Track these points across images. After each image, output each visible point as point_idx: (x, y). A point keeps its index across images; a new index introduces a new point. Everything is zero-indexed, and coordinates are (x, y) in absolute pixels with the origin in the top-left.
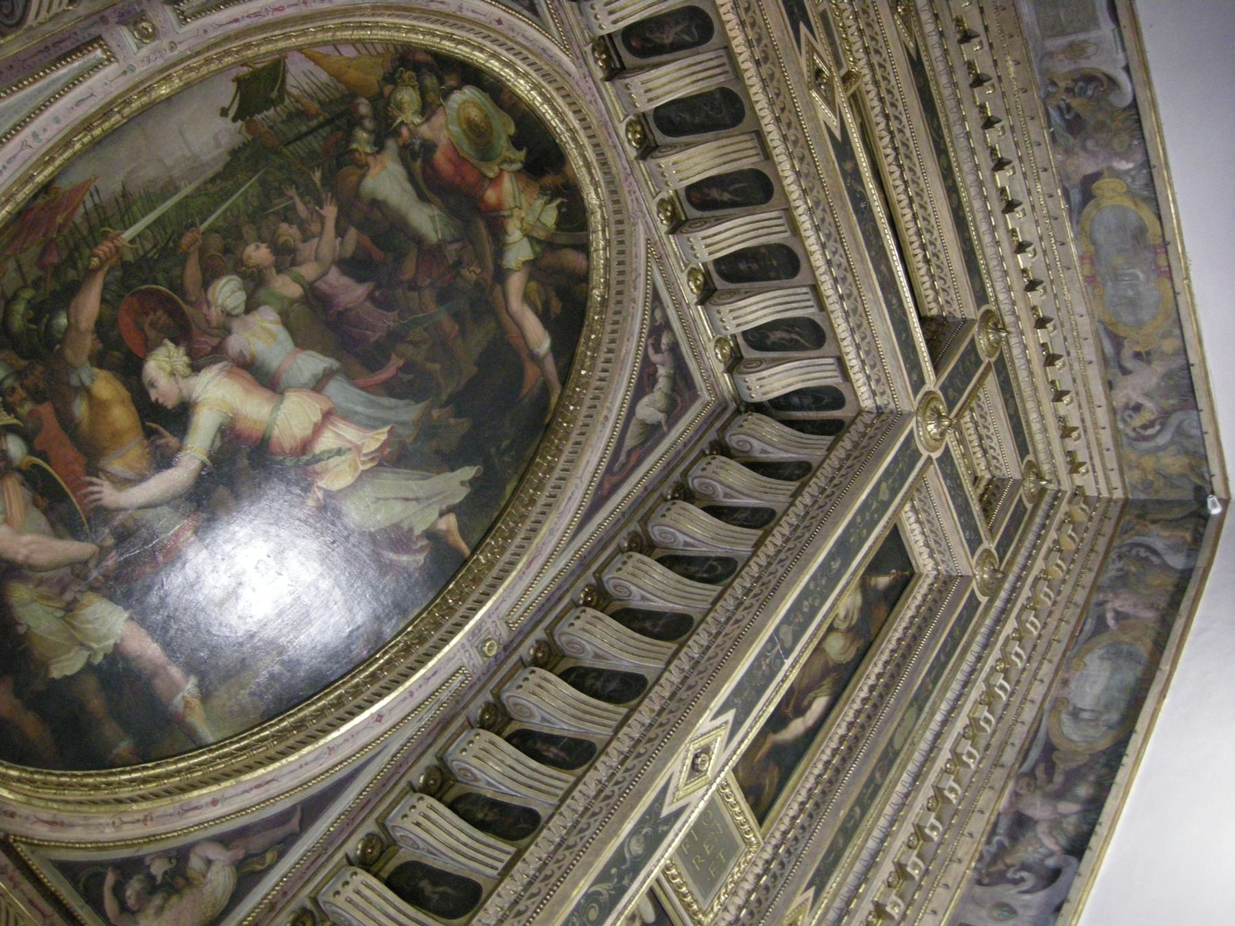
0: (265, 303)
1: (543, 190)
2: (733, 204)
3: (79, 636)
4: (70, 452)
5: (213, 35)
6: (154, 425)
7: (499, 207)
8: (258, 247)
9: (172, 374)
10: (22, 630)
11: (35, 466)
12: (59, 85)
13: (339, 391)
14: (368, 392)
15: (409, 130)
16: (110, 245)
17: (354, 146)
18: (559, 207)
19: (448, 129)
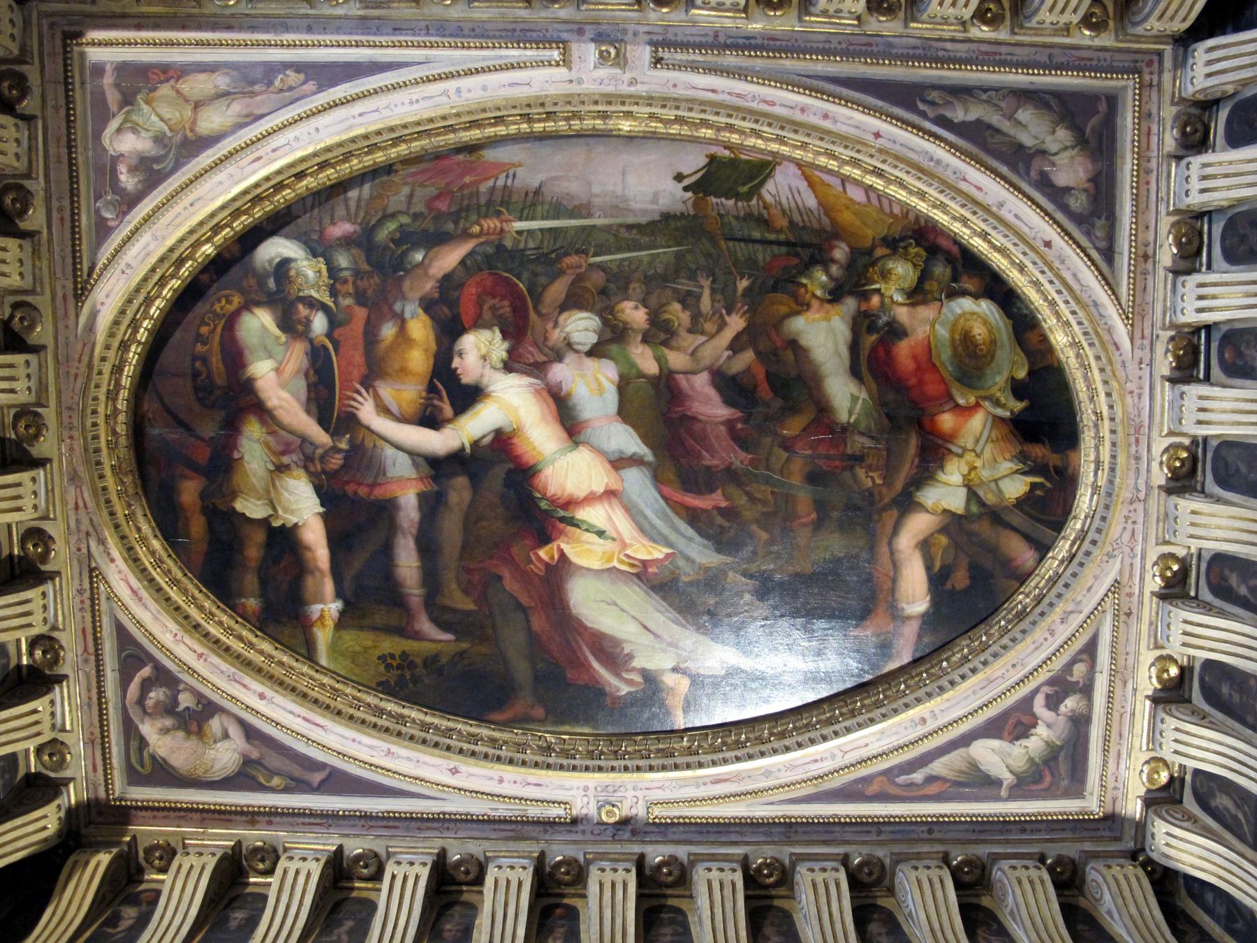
0: (611, 358)
1: (1022, 457)
2: (1245, 604)
3: (273, 495)
4: (358, 358)
5: (681, 92)
6: (440, 386)
7: (950, 438)
8: (637, 308)
9: (484, 358)
10: (236, 455)
11: (325, 348)
12: (502, 62)
13: (637, 482)
14: (667, 503)
15: (882, 303)
16: (498, 224)
17: (804, 281)
18: (1034, 486)
19: (933, 325)
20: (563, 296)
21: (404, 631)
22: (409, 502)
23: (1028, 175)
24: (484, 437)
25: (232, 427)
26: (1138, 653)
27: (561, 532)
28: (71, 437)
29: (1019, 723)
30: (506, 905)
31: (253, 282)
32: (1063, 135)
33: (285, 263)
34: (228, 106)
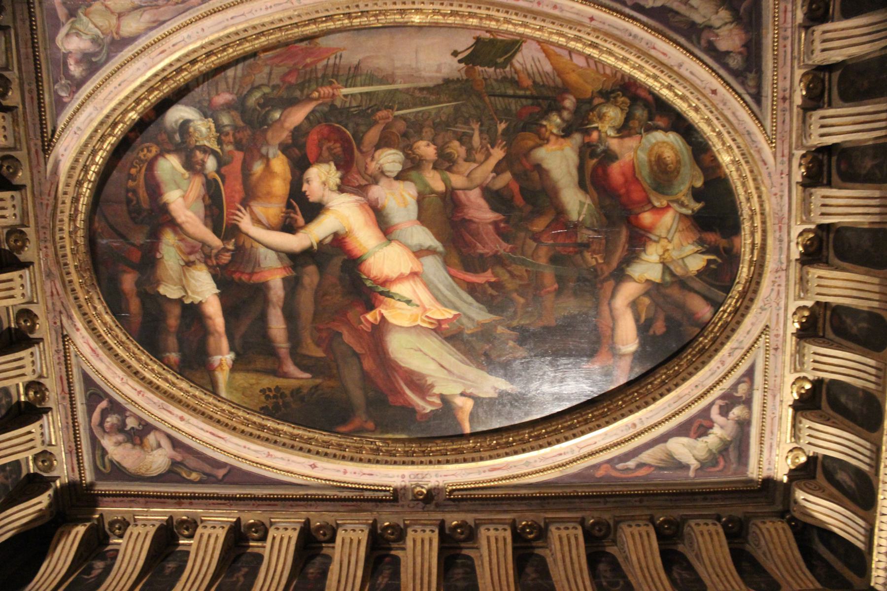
0: (411, 181)
1: (700, 242)
3: (184, 282)
4: (239, 187)
6: (295, 204)
7: (649, 230)
8: (428, 145)
9: (324, 183)
10: (158, 256)
13: (432, 266)
14: (454, 281)
15: (600, 136)
16: (331, 91)
17: (545, 123)
19: (636, 152)
20: (377, 138)
21: (277, 372)
22: (276, 283)
23: (699, 43)
24: (326, 238)
25: (155, 236)
26: (783, 376)
27: (381, 302)
28: (46, 247)
29: (701, 426)
30: (350, 555)
31: (164, 136)
32: (724, 14)
33: (186, 124)
34: (141, 16)
